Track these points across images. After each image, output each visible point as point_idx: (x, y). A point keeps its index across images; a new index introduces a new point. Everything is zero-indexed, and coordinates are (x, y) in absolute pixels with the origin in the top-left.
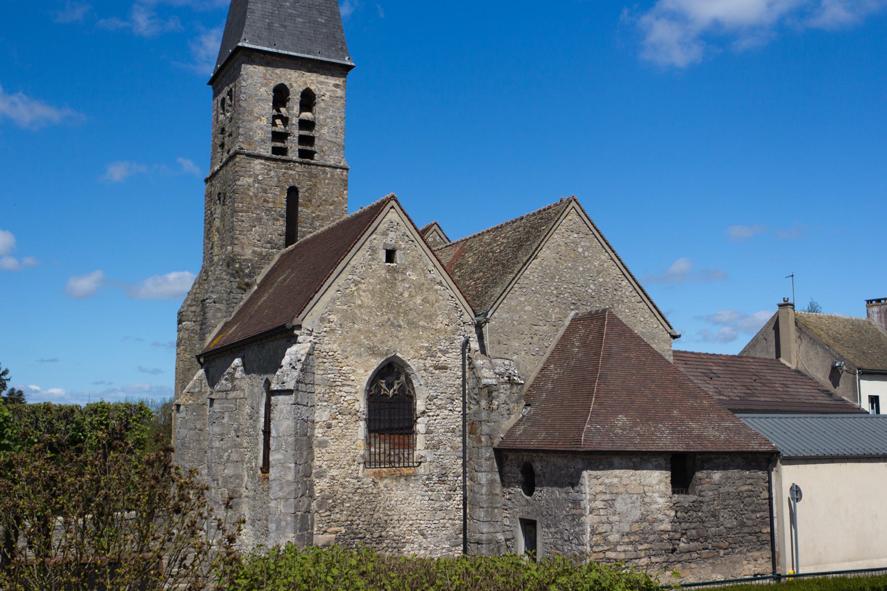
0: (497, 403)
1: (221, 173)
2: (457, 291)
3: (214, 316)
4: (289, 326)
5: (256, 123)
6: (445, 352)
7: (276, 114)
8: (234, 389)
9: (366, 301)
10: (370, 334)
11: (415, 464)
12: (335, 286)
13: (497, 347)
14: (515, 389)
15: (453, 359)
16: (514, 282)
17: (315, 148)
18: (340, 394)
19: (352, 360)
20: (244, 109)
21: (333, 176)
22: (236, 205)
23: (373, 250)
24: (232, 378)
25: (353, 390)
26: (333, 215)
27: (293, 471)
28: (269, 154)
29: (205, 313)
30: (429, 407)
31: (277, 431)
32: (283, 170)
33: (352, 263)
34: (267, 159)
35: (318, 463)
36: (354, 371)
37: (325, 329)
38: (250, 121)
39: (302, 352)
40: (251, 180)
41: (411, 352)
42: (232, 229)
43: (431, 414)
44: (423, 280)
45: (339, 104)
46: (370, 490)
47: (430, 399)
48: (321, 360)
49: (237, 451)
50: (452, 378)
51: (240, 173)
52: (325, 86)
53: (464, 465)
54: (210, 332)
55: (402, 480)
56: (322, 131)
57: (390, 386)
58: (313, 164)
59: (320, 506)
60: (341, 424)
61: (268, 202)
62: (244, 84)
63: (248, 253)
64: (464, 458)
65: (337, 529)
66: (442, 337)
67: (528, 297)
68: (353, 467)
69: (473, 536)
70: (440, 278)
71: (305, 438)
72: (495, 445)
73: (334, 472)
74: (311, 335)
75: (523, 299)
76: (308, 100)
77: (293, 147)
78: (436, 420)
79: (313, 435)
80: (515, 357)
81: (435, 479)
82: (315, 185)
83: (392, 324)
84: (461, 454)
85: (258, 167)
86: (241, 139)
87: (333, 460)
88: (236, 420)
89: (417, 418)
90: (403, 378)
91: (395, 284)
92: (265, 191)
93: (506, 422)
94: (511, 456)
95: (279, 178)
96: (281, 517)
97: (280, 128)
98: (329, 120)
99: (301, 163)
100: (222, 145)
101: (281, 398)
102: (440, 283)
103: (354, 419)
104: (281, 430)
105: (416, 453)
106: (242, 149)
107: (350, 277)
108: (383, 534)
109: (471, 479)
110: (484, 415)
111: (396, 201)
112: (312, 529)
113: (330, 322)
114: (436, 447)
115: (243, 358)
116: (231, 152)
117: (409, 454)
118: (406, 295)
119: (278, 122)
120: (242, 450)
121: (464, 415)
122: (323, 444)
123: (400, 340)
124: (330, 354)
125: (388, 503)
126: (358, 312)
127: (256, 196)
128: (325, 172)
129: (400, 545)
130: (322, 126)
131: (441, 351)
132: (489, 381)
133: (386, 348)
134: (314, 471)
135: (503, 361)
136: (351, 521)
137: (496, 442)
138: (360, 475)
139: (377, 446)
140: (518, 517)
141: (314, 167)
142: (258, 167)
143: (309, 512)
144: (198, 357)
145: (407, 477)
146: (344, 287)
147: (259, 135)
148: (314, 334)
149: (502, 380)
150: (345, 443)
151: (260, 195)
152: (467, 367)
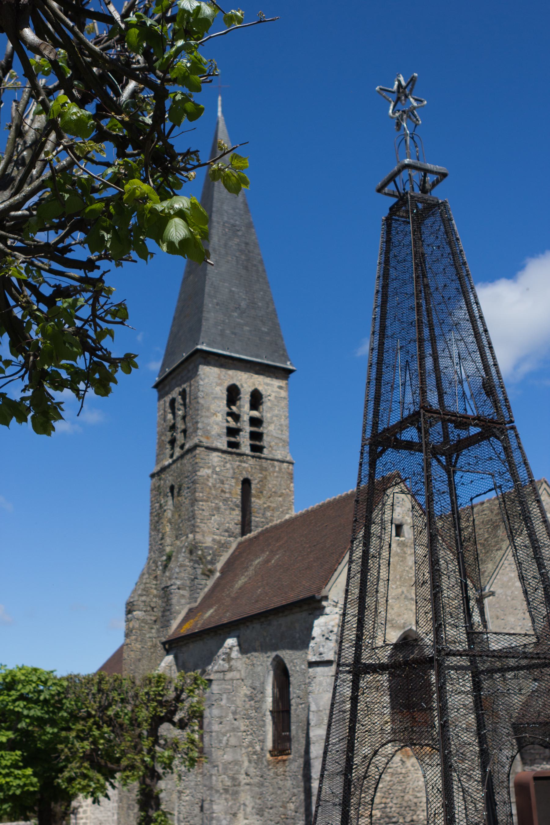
1: (174, 466)
3: (179, 602)
4: (318, 597)
7: (230, 411)
8: (230, 669)
17: (265, 443)
20: (202, 406)
21: (280, 469)
22: (197, 494)
24: (228, 659)
26: (282, 506)
28: (225, 447)
29: (168, 600)
31: (317, 704)
32: (238, 463)
34: (224, 452)
39: (332, 623)
40: (209, 471)
42: (194, 517)
45: (284, 403)
49: (235, 735)
51: (201, 465)
52: (270, 387)
54: (175, 618)
56: (270, 428)
58: (264, 458)
61: (225, 492)
62: (201, 383)
63: (208, 541)
74: (336, 606)
76: (256, 399)
82: (265, 478)
83: (406, 598)
86: (200, 433)
88: (233, 702)
91: (405, 558)
92: (222, 482)
95: (234, 469)
98: (275, 418)
99: (253, 457)
100: (173, 442)
101: (319, 670)
104: (322, 703)
106: (201, 442)
115: (238, 637)
116: (187, 447)
119: (230, 419)
120: (240, 734)
125: (416, 784)
128: (273, 466)
130: (270, 423)
133: (403, 621)
141: (264, 461)
144: (164, 644)
151: (218, 485)
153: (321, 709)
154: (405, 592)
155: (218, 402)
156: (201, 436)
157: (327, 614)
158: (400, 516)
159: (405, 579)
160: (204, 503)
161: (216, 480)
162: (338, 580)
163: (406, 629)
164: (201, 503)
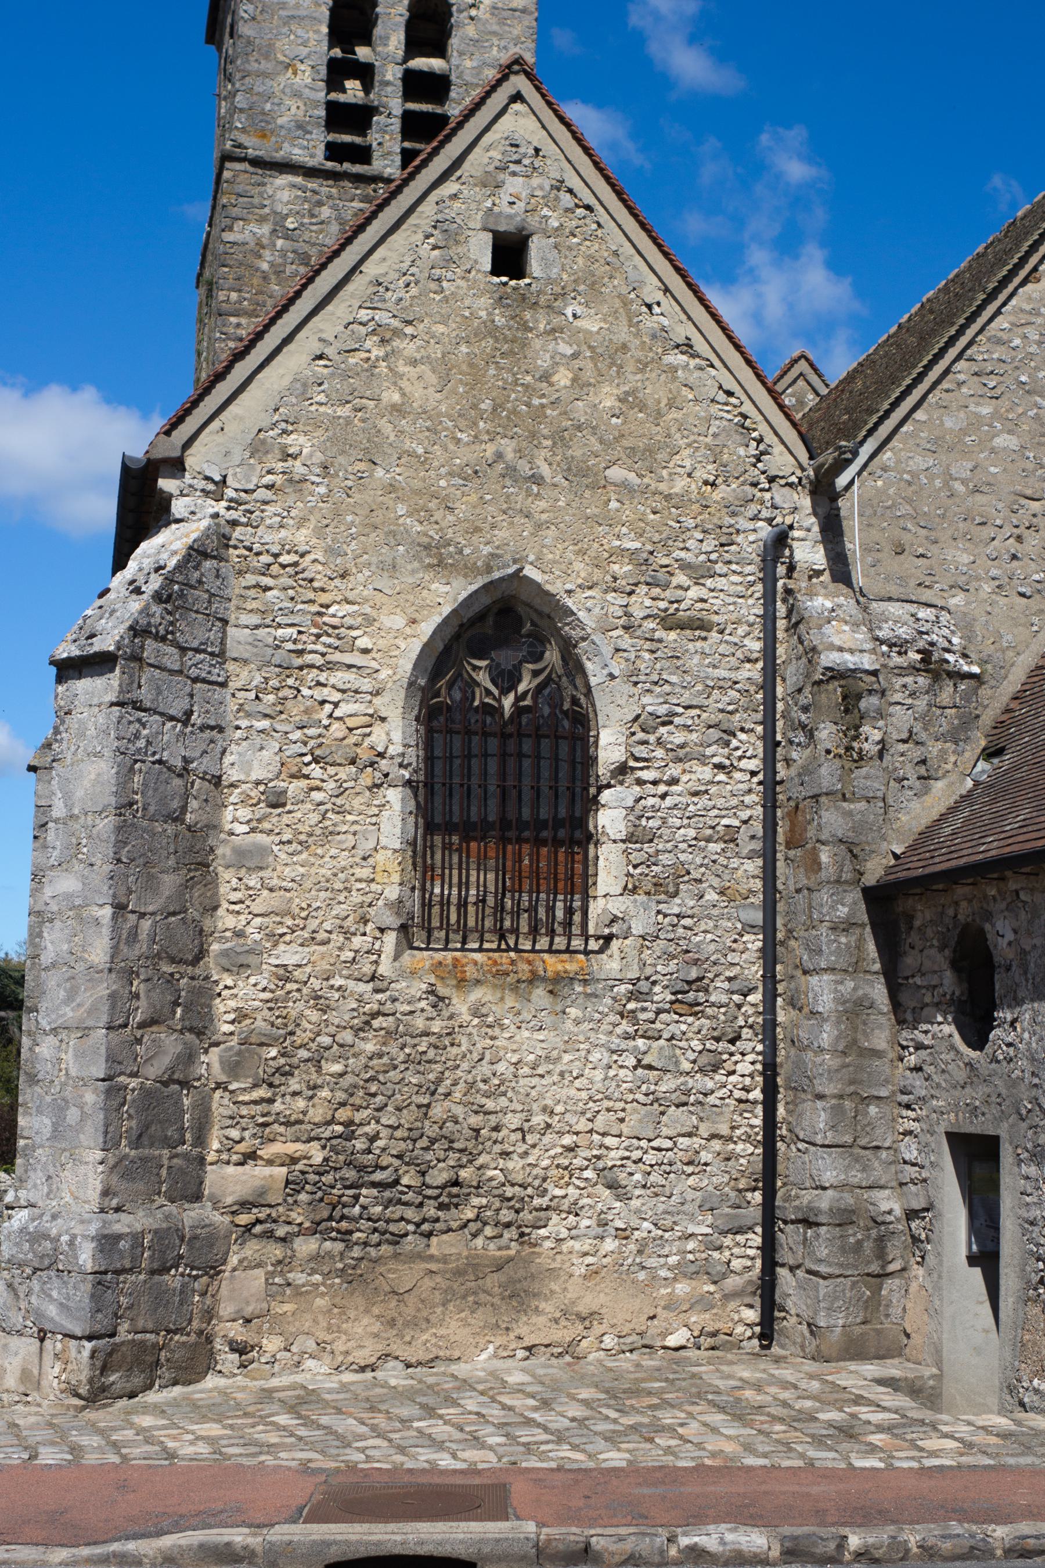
0: (877, 735)
2: (746, 375)
5: (282, 79)
6: (700, 573)
9: (417, 392)
10: (428, 502)
11: (593, 945)
12: (307, 343)
13: (893, 565)
14: (947, 693)
15: (733, 597)
16: (952, 353)
18: (319, 694)
19: (359, 584)
22: (222, 296)
23: (448, 234)
25: (366, 684)
27: (106, 931)
28: (317, 158)
30: (641, 751)
31: (67, 797)
33: (371, 268)
34: (311, 173)
35: (230, 922)
36: (370, 621)
37: (269, 479)
38: (264, 75)
40: (265, 230)
41: (578, 566)
43: (646, 775)
44: (623, 333)
46: (420, 1023)
47: (644, 724)
48: (251, 579)
50: (727, 660)
51: (235, 212)
53: (769, 955)
55: (539, 993)
57: (507, 680)
59: (234, 1068)
60: (317, 796)
64: (769, 928)
65: (292, 1148)
66: (691, 523)
67: (1004, 403)
68: (357, 941)
69: (793, 1200)
70: (683, 331)
71: (170, 828)
72: (870, 880)
73: (289, 955)
75: (986, 410)
77: (386, 140)
78: (668, 797)
79: (214, 827)
80: (957, 600)
81: (662, 995)
84: (757, 917)
85: (285, 195)
87: (288, 913)
89: (600, 789)
90: (552, 656)
91: (525, 344)
93: (915, 805)
94: (923, 914)
96: (68, 1093)
97: (353, 91)
102: (687, 347)
103: (367, 778)
104: (79, 793)
105: (596, 908)
106: (240, 146)
107: (364, 315)
108: (464, 1174)
109: (792, 1003)
110: (828, 775)
111: (529, 76)
112: (201, 1140)
113: (286, 456)
114: (664, 888)
117: (569, 911)
118: (563, 378)
121: (771, 785)
122: (250, 860)
123: (539, 526)
124: (285, 559)
125: (485, 1069)
126: (388, 429)
127: (278, 273)
129: (526, 1216)
131: (685, 566)
132: (850, 660)
133: (487, 550)
134: (215, 947)
135: (912, 608)
136: (348, 1123)
137: (874, 871)
140: (941, 1129)
142: (285, 195)
143: (184, 1084)
145: (556, 985)
146: (338, 345)
147: (291, 111)
148: (230, 493)
149: (897, 660)
150: (331, 860)
151: (290, 269)
152: (781, 624)
153: (76, 811)
154: (510, 455)
155: (300, 32)
156: (243, 130)
157: (178, 521)
158: (520, 206)
159: (514, 411)
160: (243, 321)
161: (283, 253)
162: (232, 409)
163: (497, 575)
164: (233, 320)
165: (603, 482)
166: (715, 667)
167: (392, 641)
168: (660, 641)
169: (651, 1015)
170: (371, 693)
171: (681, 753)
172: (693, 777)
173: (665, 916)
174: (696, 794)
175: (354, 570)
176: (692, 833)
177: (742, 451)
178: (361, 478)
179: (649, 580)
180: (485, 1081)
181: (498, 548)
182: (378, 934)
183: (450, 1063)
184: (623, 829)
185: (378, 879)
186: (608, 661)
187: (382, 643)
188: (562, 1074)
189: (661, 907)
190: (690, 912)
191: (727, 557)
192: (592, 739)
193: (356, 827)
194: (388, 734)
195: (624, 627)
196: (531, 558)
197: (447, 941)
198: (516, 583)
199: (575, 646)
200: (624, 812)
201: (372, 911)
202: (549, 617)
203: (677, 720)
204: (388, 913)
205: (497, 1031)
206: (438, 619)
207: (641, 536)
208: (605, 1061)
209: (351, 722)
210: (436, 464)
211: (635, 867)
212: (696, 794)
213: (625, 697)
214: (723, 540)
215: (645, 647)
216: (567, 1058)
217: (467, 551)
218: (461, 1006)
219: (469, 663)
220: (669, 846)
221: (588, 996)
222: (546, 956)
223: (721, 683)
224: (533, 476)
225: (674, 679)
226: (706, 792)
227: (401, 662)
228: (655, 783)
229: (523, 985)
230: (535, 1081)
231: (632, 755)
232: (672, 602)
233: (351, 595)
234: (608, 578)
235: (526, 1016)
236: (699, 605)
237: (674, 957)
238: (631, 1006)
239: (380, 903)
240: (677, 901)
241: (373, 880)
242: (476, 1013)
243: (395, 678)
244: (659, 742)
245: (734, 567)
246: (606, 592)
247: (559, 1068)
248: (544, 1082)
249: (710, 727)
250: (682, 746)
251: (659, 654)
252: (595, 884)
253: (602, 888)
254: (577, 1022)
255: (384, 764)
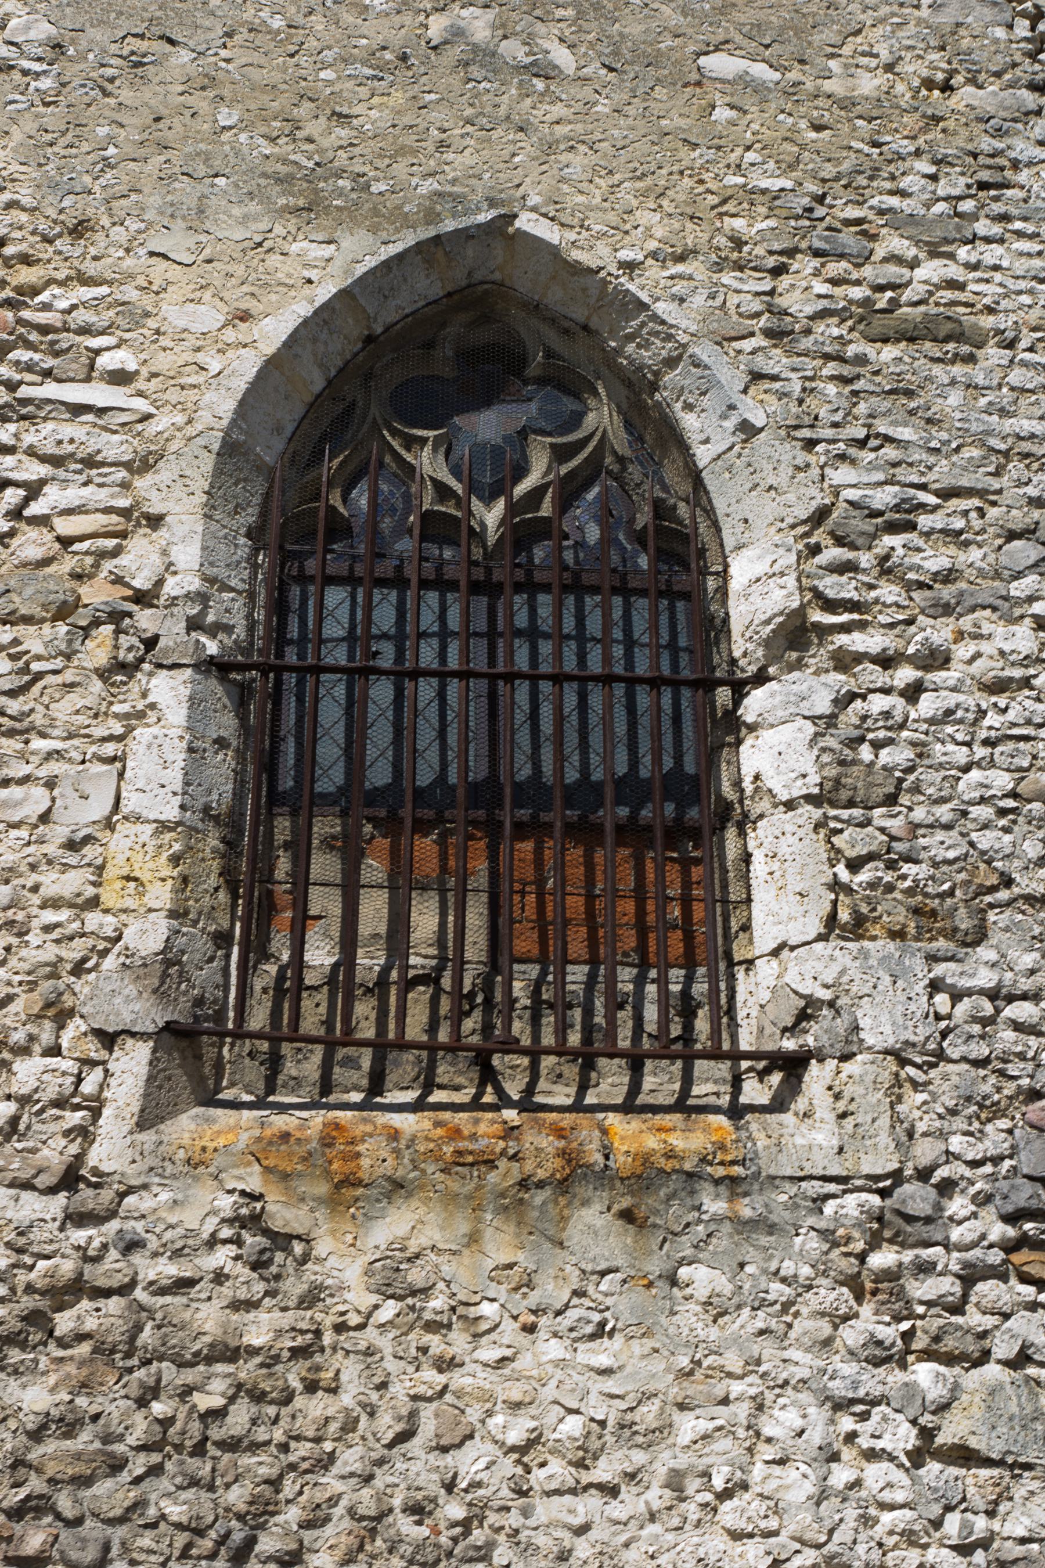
25: (114, 447)
46: (208, 1318)
55: (593, 1227)
89: (740, 689)
90: (601, 417)
103: (98, 650)
123: (550, 148)
125: (418, 1468)
133: (429, 186)
138: (110, 1151)
139: (325, 902)
145: (644, 1194)
163: (449, 225)
165: (694, 77)
166: (1003, 413)
167: (188, 357)
168: (861, 360)
169: (947, 1286)
170: (127, 465)
171: (946, 593)
172: (985, 647)
173: (957, 997)
174: (998, 687)
175: (105, 221)
176: (1002, 781)
177: (1000, 33)
178: (142, 64)
179: (818, 244)
180: (418, 1511)
181: (454, 182)
182: (93, 1049)
183: (301, 1450)
184: (811, 769)
185: (109, 897)
186: (737, 398)
187: (163, 362)
188: (675, 1482)
189: (940, 969)
190: (1025, 984)
191: (998, 208)
192: (711, 583)
193: (55, 767)
194: (165, 553)
195: (768, 333)
196: (534, 200)
197: (326, 1086)
198: (499, 251)
199: (654, 387)
200: (810, 729)
201: (83, 986)
202: (585, 328)
203: (924, 521)
204: (131, 990)
205: (458, 1341)
206: (304, 310)
207: (792, 167)
208: (816, 1436)
209: (65, 526)
210: (312, 44)
211: (855, 865)
212: (998, 687)
213: (786, 471)
214: (985, 175)
215: (825, 372)
216: (689, 1426)
217: (377, 187)
218: (344, 1262)
219: (394, 433)
220: (944, 813)
221: (745, 1227)
222: (612, 1119)
223: (1026, 446)
224: (534, 64)
225: (905, 433)
226: (1026, 683)
227: (209, 397)
228: (886, 661)
229: (540, 1197)
230: (588, 1506)
231: (818, 595)
232: (880, 288)
233: (91, 268)
234: (722, 241)
235: (552, 1291)
236: (948, 295)
237: (997, 1112)
238: (882, 1259)
239: (110, 963)
240: (985, 953)
241: (94, 903)
242: (391, 1279)
243: (190, 431)
244: (886, 568)
245: (1018, 225)
246: (718, 267)
247: (665, 1462)
248: (617, 1510)
249: (1012, 536)
250: (948, 576)
251: (860, 385)
252: (746, 927)
253: (765, 933)
254: (717, 1310)
255: (146, 620)
